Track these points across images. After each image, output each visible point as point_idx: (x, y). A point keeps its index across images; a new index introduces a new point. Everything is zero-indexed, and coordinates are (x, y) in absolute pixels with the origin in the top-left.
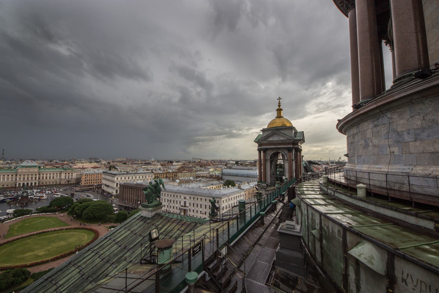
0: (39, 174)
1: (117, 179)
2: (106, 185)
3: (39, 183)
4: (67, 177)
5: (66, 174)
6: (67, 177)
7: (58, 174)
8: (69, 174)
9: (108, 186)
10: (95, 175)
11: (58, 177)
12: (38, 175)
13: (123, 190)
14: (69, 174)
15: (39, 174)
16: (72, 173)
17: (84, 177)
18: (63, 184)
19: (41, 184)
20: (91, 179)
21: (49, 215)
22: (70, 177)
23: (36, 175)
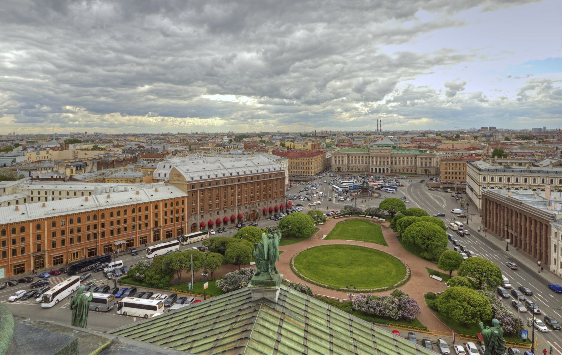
0: (392, 158)
2: (469, 186)
3: (392, 170)
4: (424, 164)
5: (422, 159)
6: (424, 164)
7: (413, 158)
9: (472, 190)
11: (413, 163)
12: (390, 159)
13: (486, 205)
14: (426, 159)
15: (392, 158)
16: (430, 159)
20: (454, 171)
22: (428, 165)
23: (388, 158)
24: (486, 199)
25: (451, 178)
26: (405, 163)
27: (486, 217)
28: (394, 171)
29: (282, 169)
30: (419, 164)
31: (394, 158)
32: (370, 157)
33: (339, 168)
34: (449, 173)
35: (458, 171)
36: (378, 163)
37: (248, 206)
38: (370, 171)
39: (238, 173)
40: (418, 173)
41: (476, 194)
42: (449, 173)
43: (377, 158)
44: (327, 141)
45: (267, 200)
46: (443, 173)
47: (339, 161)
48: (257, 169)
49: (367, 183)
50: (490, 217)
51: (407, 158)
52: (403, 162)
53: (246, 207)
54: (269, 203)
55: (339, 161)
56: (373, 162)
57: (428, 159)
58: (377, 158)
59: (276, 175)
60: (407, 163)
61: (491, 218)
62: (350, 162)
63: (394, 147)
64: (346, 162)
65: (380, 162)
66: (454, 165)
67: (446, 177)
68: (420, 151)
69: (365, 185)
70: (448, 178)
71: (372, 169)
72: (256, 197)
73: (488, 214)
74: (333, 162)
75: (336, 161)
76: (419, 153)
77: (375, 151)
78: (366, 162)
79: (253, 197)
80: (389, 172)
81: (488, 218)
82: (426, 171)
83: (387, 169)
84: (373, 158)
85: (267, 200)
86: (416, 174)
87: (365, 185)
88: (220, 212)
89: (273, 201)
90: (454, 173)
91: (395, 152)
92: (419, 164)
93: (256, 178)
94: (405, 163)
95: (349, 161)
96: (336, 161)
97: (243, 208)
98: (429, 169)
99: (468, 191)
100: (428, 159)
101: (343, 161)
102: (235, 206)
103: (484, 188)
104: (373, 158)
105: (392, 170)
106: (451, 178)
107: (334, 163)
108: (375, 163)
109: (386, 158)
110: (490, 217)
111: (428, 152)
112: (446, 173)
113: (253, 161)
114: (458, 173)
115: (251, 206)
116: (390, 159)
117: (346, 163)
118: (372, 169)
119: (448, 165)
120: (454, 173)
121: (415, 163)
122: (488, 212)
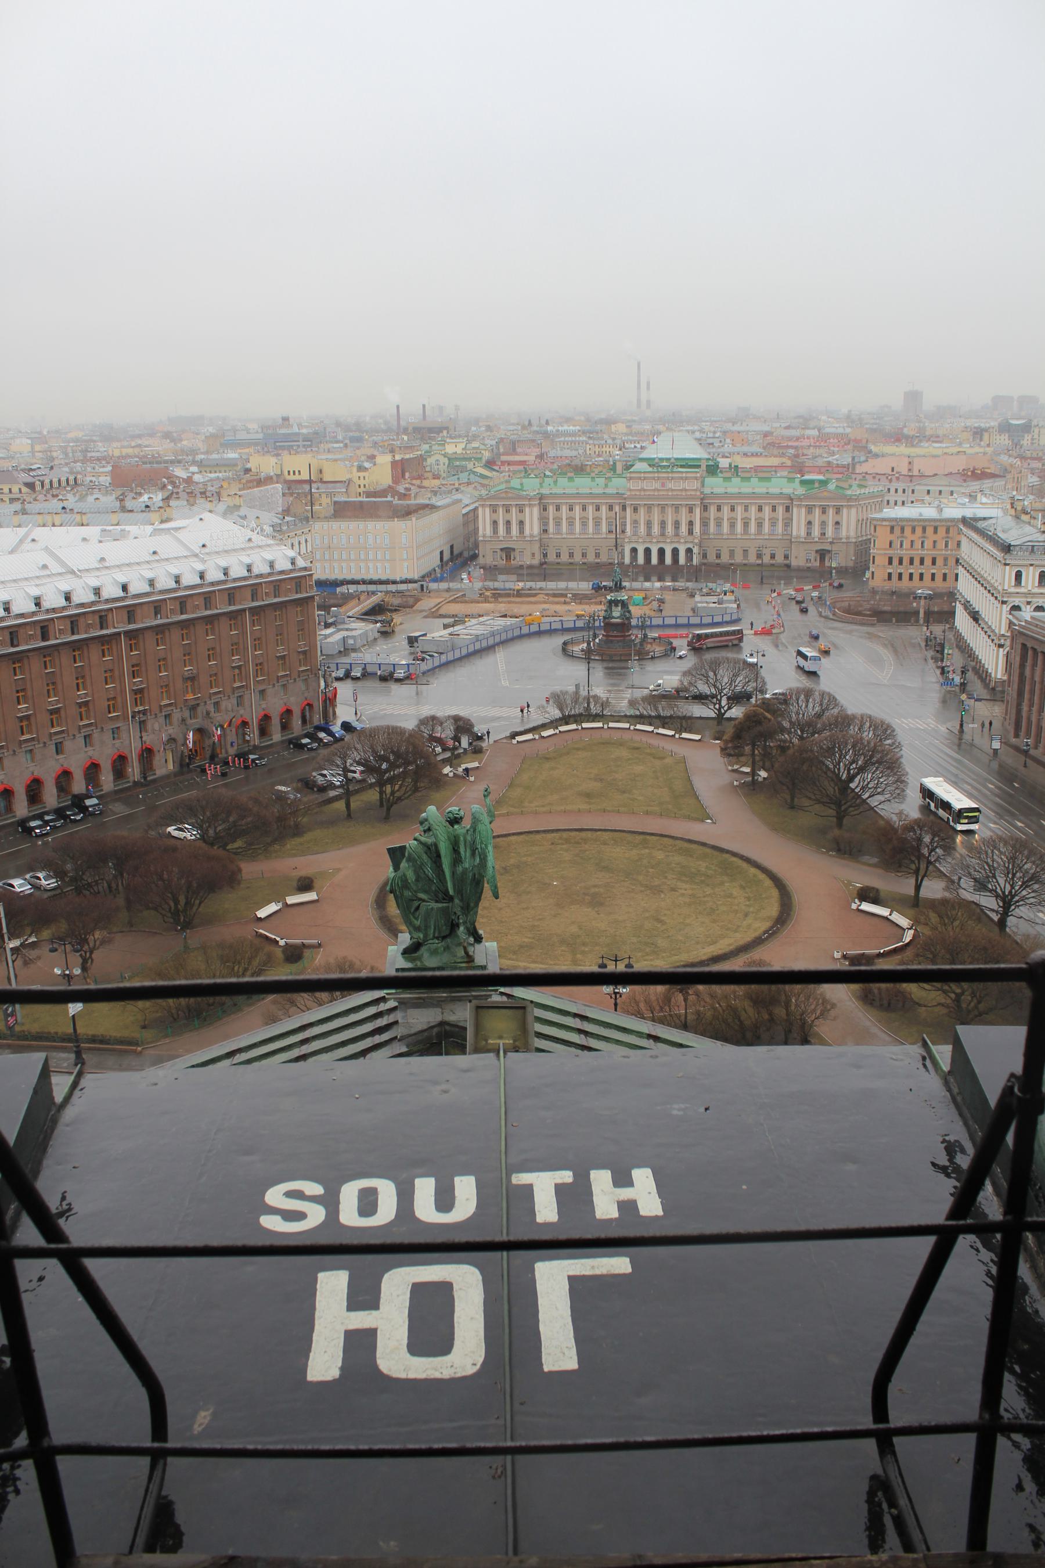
0: (705, 508)
1: (1018, 576)
2: (967, 605)
4: (816, 532)
5: (810, 509)
6: (816, 532)
7: (780, 510)
8: (824, 511)
9: (975, 616)
10: (942, 531)
11: (780, 528)
12: (697, 511)
13: (1022, 666)
14: (824, 511)
15: (705, 508)
16: (838, 510)
17: (882, 538)
18: (799, 569)
19: (712, 558)
20: (917, 553)
21: (645, 738)
22: (830, 532)
23: (691, 510)
24: (1024, 646)
25: (906, 577)
26: (753, 528)
27: (1019, 705)
28: (712, 558)
29: (301, 563)
30: (798, 529)
31: (713, 509)
32: (624, 508)
33: (508, 552)
34: (901, 562)
35: (928, 553)
36: (656, 529)
37: (177, 716)
38: (627, 560)
39: (125, 588)
40: (794, 563)
41: (989, 632)
42: (901, 562)
43: (649, 508)
44: (450, 449)
45: (246, 687)
46: (881, 561)
47: (508, 523)
48: (200, 567)
49: (624, 604)
50: (1031, 705)
51: (760, 509)
52: (746, 525)
53: (168, 717)
54: (254, 697)
55: (508, 523)
56: (635, 522)
57: (831, 512)
58: (649, 508)
59: (277, 586)
60: (760, 525)
61: (1035, 709)
62: (551, 528)
63: (713, 469)
64: (533, 527)
65: (663, 524)
66: (919, 531)
67: (890, 574)
68: (803, 483)
69: (617, 612)
70: (895, 577)
71: (634, 551)
72: (204, 679)
73: (1026, 696)
74: (484, 529)
75: (495, 523)
76: (800, 491)
77: (645, 485)
78: (609, 524)
79: (192, 679)
80: (695, 562)
81: (1025, 708)
82: (822, 554)
83: (689, 551)
84: (635, 510)
85: (246, 687)
86: (788, 566)
87: (617, 612)
88: (68, 745)
89: (270, 691)
90: (917, 562)
91: (715, 485)
92: (798, 529)
93: (199, 601)
94: (753, 528)
95: (544, 521)
96: (495, 523)
97: (154, 723)
98: (835, 548)
99: (962, 620)
100: (831, 512)
101: (521, 523)
102: (125, 718)
103: (1016, 608)
104: (635, 510)
105: (705, 556)
106: (906, 577)
107: (489, 531)
108: (642, 529)
109: (684, 511)
110: (1031, 705)
111: (832, 486)
112: (890, 562)
113: (179, 535)
114: (928, 562)
115: (187, 714)
116: (697, 511)
117: (536, 531)
118: (634, 551)
119: (897, 530)
120: (917, 562)
121: (788, 523)
122: (1027, 688)
